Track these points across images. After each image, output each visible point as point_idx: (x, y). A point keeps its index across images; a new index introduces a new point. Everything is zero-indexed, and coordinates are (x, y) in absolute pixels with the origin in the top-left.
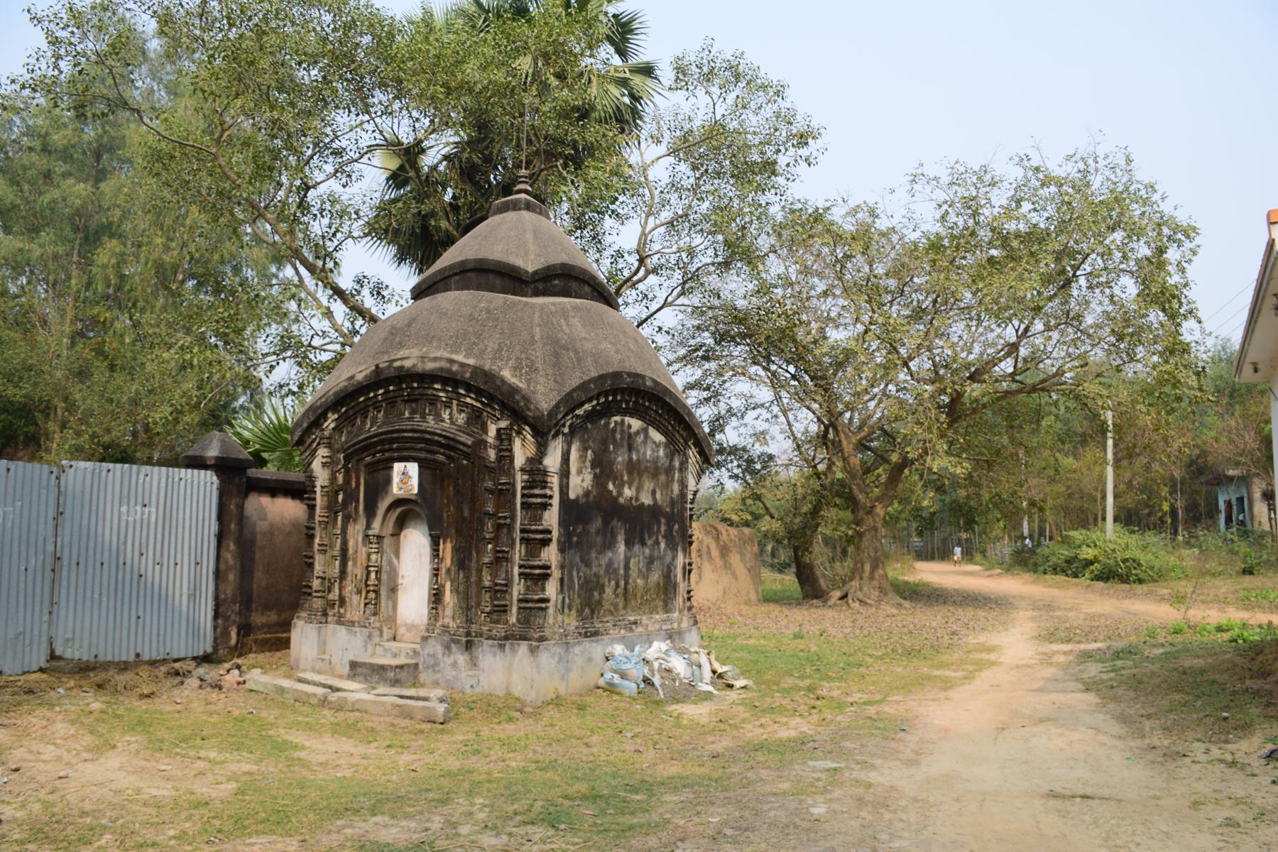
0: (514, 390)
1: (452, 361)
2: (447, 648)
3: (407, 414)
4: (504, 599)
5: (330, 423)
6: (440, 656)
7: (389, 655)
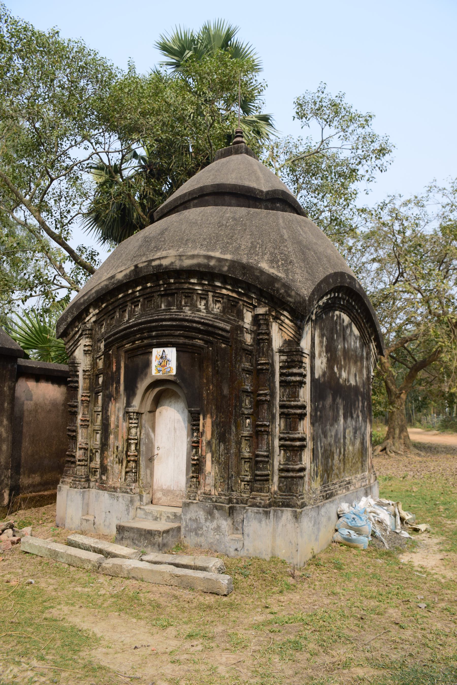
0: (273, 279)
1: (209, 258)
2: (210, 513)
3: (163, 307)
4: (266, 469)
5: (91, 317)
6: (203, 521)
7: (150, 517)
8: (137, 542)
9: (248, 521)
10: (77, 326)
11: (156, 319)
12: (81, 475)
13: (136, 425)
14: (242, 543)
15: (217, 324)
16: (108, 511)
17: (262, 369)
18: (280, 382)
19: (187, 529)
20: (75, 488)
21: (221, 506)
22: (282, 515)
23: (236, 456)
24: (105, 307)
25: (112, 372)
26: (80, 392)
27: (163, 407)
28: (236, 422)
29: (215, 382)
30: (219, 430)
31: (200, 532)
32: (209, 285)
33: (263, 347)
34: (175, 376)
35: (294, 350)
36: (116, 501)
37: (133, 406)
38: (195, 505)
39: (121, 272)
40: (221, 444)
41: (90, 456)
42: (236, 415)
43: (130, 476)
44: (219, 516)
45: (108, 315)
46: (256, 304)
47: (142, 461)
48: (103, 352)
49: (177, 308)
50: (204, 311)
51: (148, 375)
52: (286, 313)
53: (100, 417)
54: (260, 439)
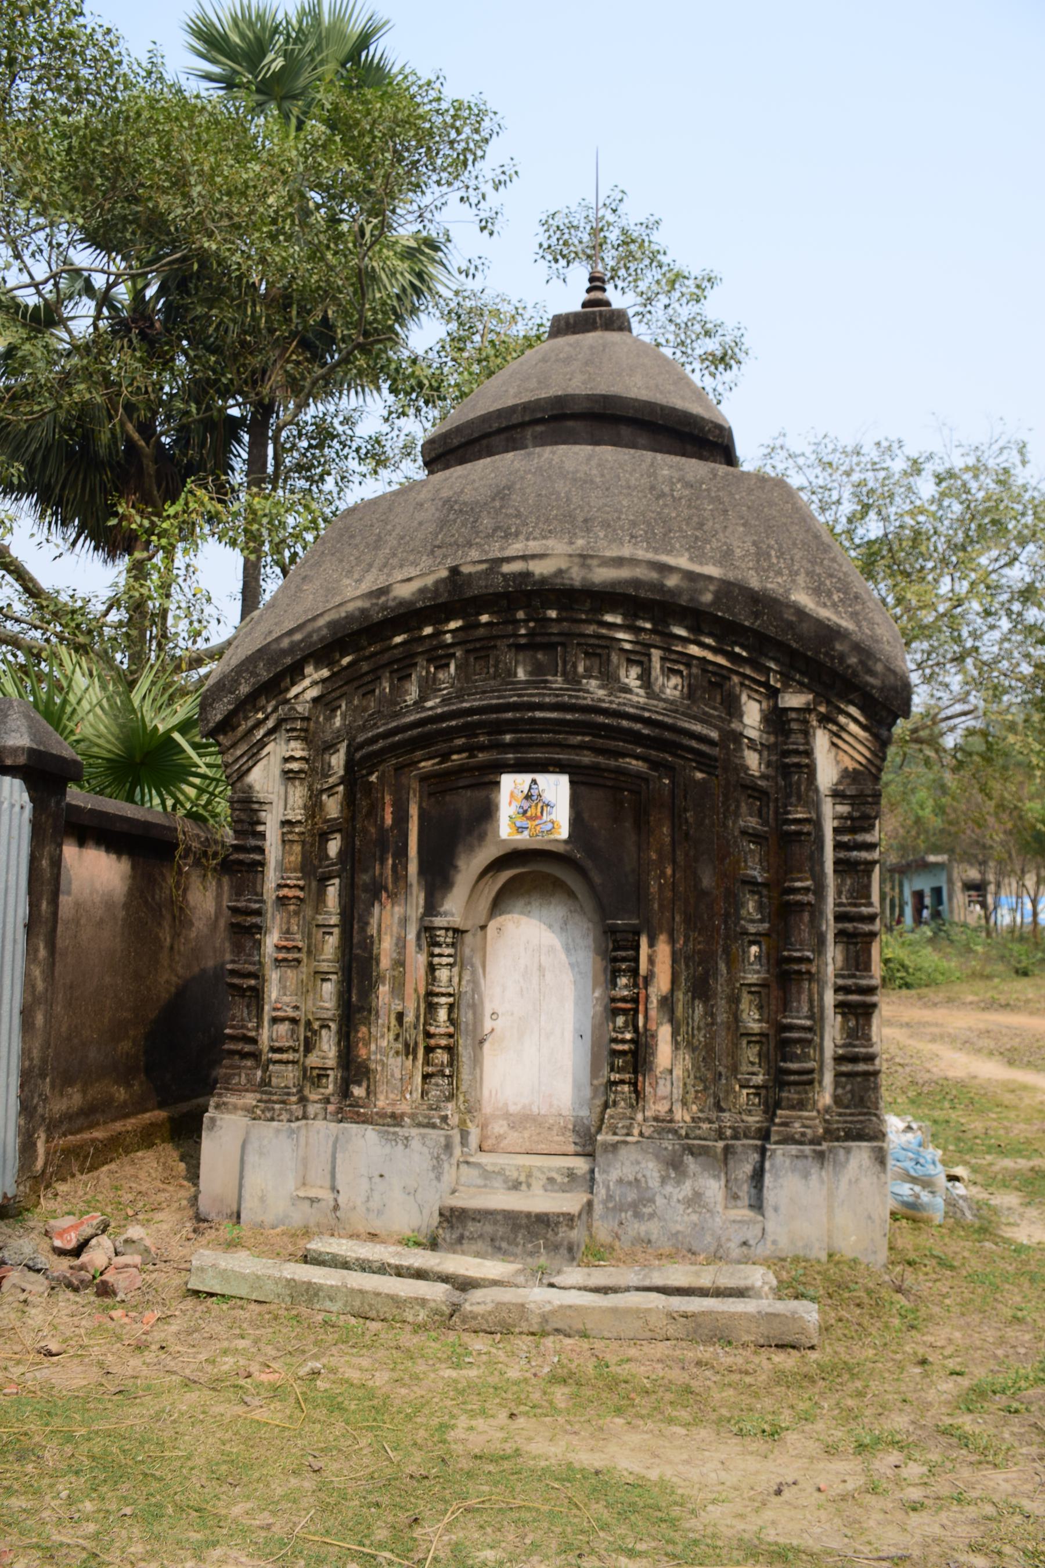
0: (830, 633)
1: (665, 569)
2: (674, 1165)
3: (521, 675)
4: (805, 1057)
5: (306, 689)
6: (654, 1183)
7: (498, 1183)
8: (504, 1245)
9: (776, 1177)
10: (263, 709)
11: (515, 704)
12: (286, 1087)
13: (451, 960)
14: (759, 1226)
15: (686, 725)
16: (376, 1174)
17: (799, 833)
18: (835, 863)
19: (611, 1205)
20: (272, 1119)
21: (703, 1146)
22: (847, 1160)
23: (729, 1029)
24: (350, 664)
25: (381, 828)
26: (271, 877)
27: (509, 916)
28: (727, 951)
29: (680, 858)
30: (691, 971)
31: (647, 1210)
32: (652, 631)
33: (799, 783)
34: (566, 842)
35: (869, 792)
36: (400, 1147)
37: (446, 914)
38: (633, 1148)
39: (409, 580)
40: (696, 1002)
41: (306, 1038)
42: (727, 937)
43: (437, 1085)
44: (699, 1169)
45: (356, 684)
46: (778, 685)
47: (466, 1047)
48: (342, 777)
49: (566, 681)
50: (641, 692)
51: (489, 837)
52: (853, 710)
53: (332, 941)
54: (794, 990)
